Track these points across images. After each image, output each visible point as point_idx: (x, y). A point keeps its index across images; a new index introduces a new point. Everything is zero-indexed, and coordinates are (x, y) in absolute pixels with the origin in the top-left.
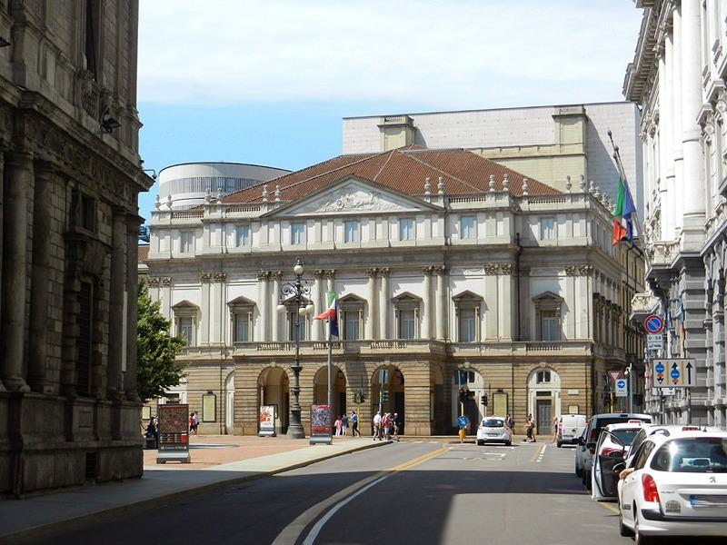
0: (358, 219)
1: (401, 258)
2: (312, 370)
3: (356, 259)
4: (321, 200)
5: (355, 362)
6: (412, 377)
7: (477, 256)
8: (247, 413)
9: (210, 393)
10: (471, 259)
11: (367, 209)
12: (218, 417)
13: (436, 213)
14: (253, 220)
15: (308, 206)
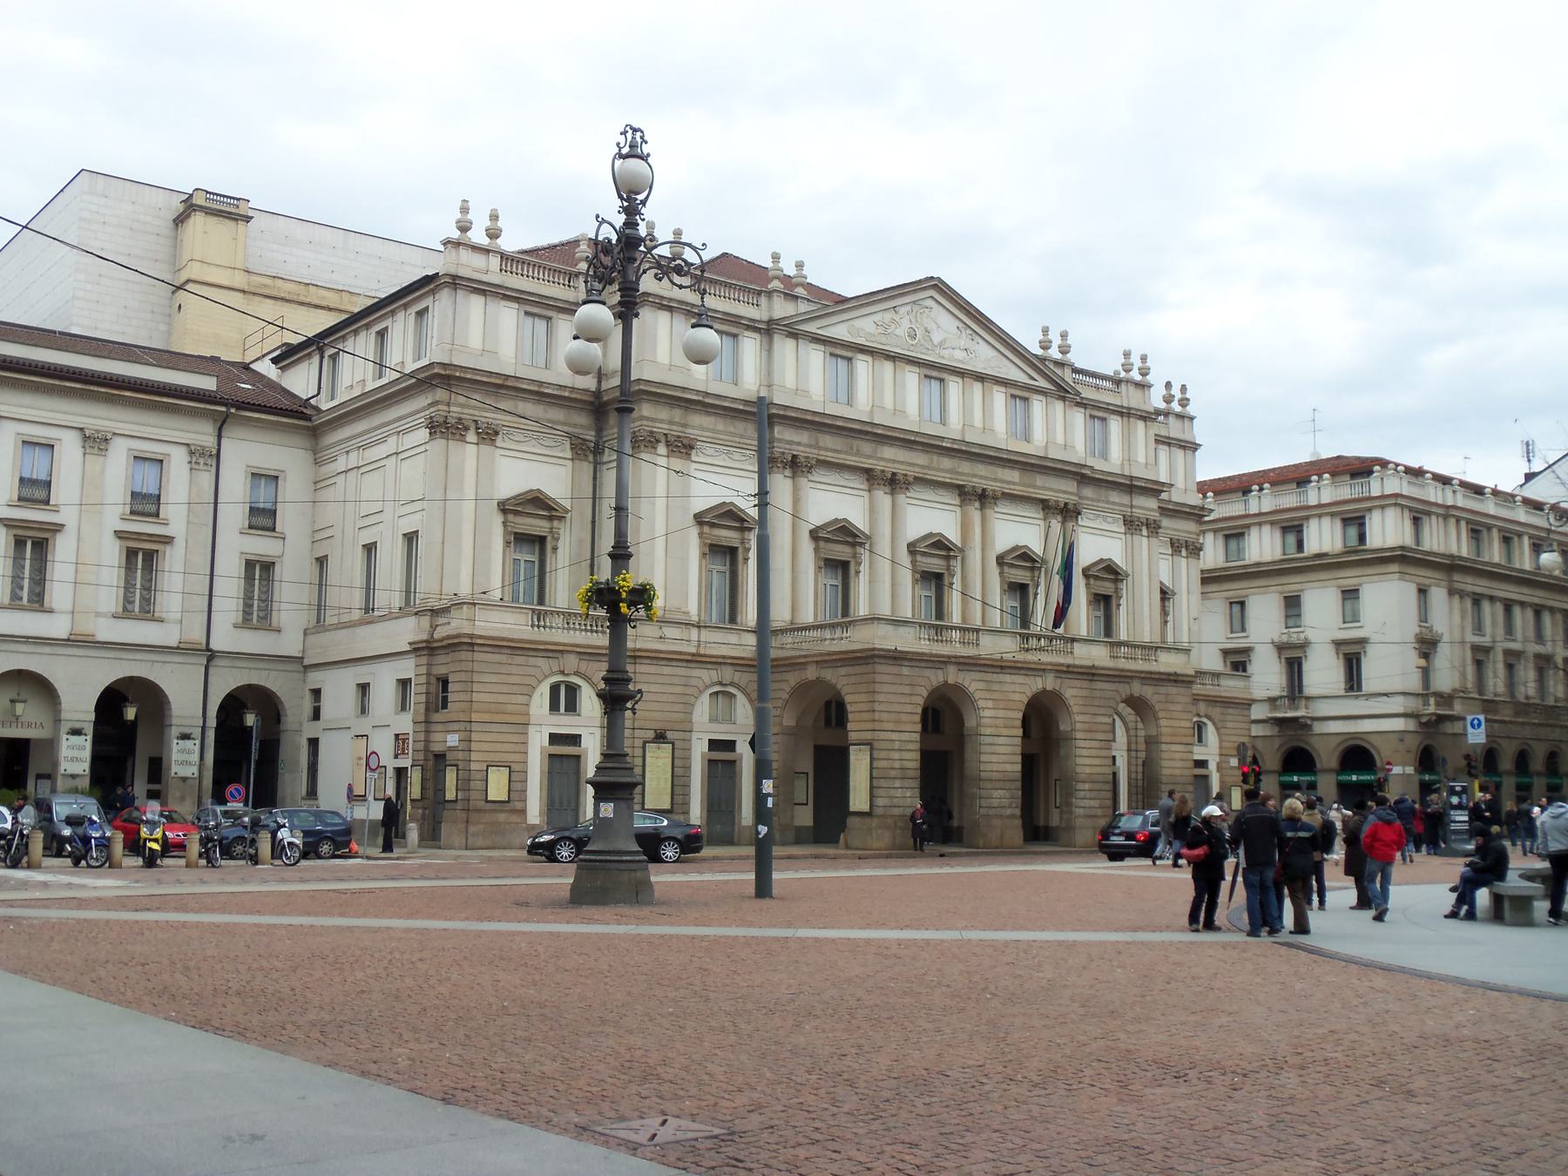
0: (944, 376)
1: (1014, 475)
2: (1017, 697)
3: (946, 463)
4: (877, 317)
5: (1085, 684)
6: (1170, 723)
7: (1115, 497)
8: (899, 793)
9: (660, 737)
10: (1108, 502)
11: (955, 357)
12: (678, 799)
13: (1063, 399)
14: (752, 326)
15: (858, 323)
